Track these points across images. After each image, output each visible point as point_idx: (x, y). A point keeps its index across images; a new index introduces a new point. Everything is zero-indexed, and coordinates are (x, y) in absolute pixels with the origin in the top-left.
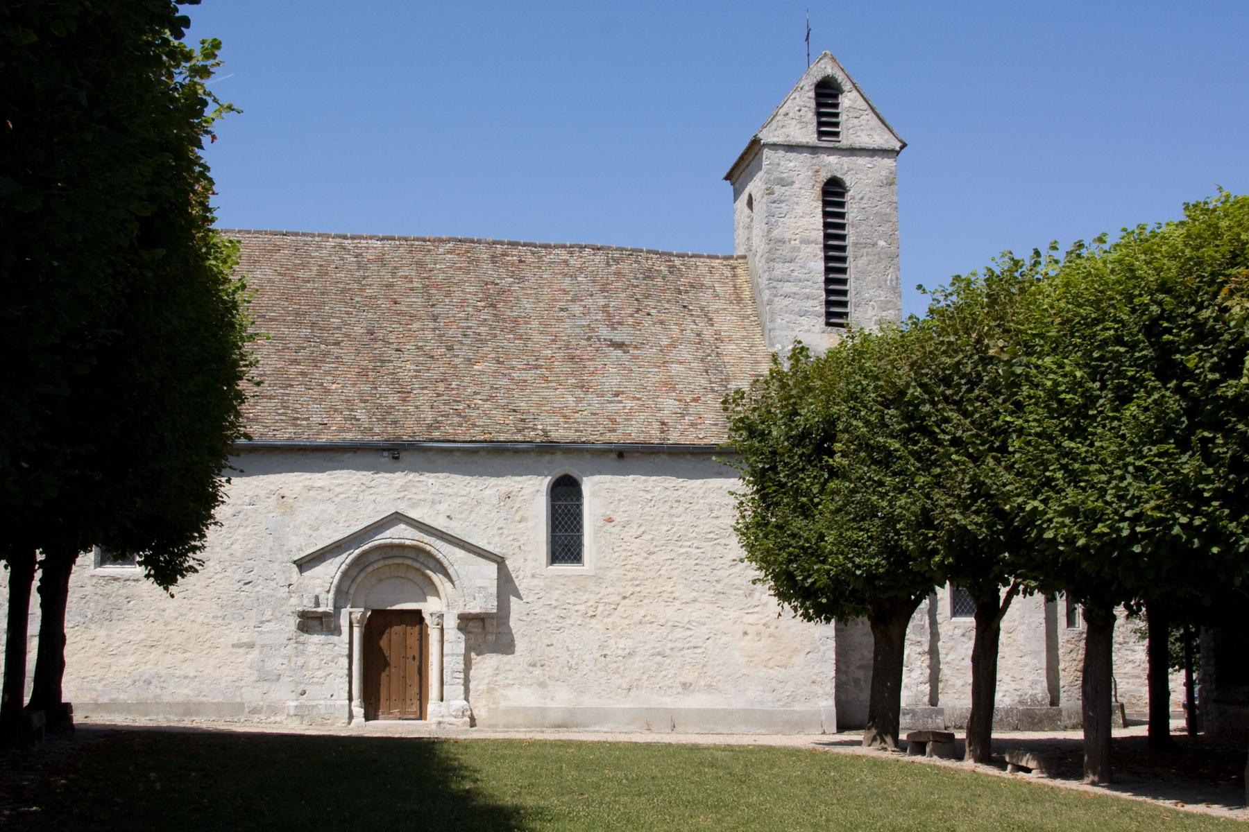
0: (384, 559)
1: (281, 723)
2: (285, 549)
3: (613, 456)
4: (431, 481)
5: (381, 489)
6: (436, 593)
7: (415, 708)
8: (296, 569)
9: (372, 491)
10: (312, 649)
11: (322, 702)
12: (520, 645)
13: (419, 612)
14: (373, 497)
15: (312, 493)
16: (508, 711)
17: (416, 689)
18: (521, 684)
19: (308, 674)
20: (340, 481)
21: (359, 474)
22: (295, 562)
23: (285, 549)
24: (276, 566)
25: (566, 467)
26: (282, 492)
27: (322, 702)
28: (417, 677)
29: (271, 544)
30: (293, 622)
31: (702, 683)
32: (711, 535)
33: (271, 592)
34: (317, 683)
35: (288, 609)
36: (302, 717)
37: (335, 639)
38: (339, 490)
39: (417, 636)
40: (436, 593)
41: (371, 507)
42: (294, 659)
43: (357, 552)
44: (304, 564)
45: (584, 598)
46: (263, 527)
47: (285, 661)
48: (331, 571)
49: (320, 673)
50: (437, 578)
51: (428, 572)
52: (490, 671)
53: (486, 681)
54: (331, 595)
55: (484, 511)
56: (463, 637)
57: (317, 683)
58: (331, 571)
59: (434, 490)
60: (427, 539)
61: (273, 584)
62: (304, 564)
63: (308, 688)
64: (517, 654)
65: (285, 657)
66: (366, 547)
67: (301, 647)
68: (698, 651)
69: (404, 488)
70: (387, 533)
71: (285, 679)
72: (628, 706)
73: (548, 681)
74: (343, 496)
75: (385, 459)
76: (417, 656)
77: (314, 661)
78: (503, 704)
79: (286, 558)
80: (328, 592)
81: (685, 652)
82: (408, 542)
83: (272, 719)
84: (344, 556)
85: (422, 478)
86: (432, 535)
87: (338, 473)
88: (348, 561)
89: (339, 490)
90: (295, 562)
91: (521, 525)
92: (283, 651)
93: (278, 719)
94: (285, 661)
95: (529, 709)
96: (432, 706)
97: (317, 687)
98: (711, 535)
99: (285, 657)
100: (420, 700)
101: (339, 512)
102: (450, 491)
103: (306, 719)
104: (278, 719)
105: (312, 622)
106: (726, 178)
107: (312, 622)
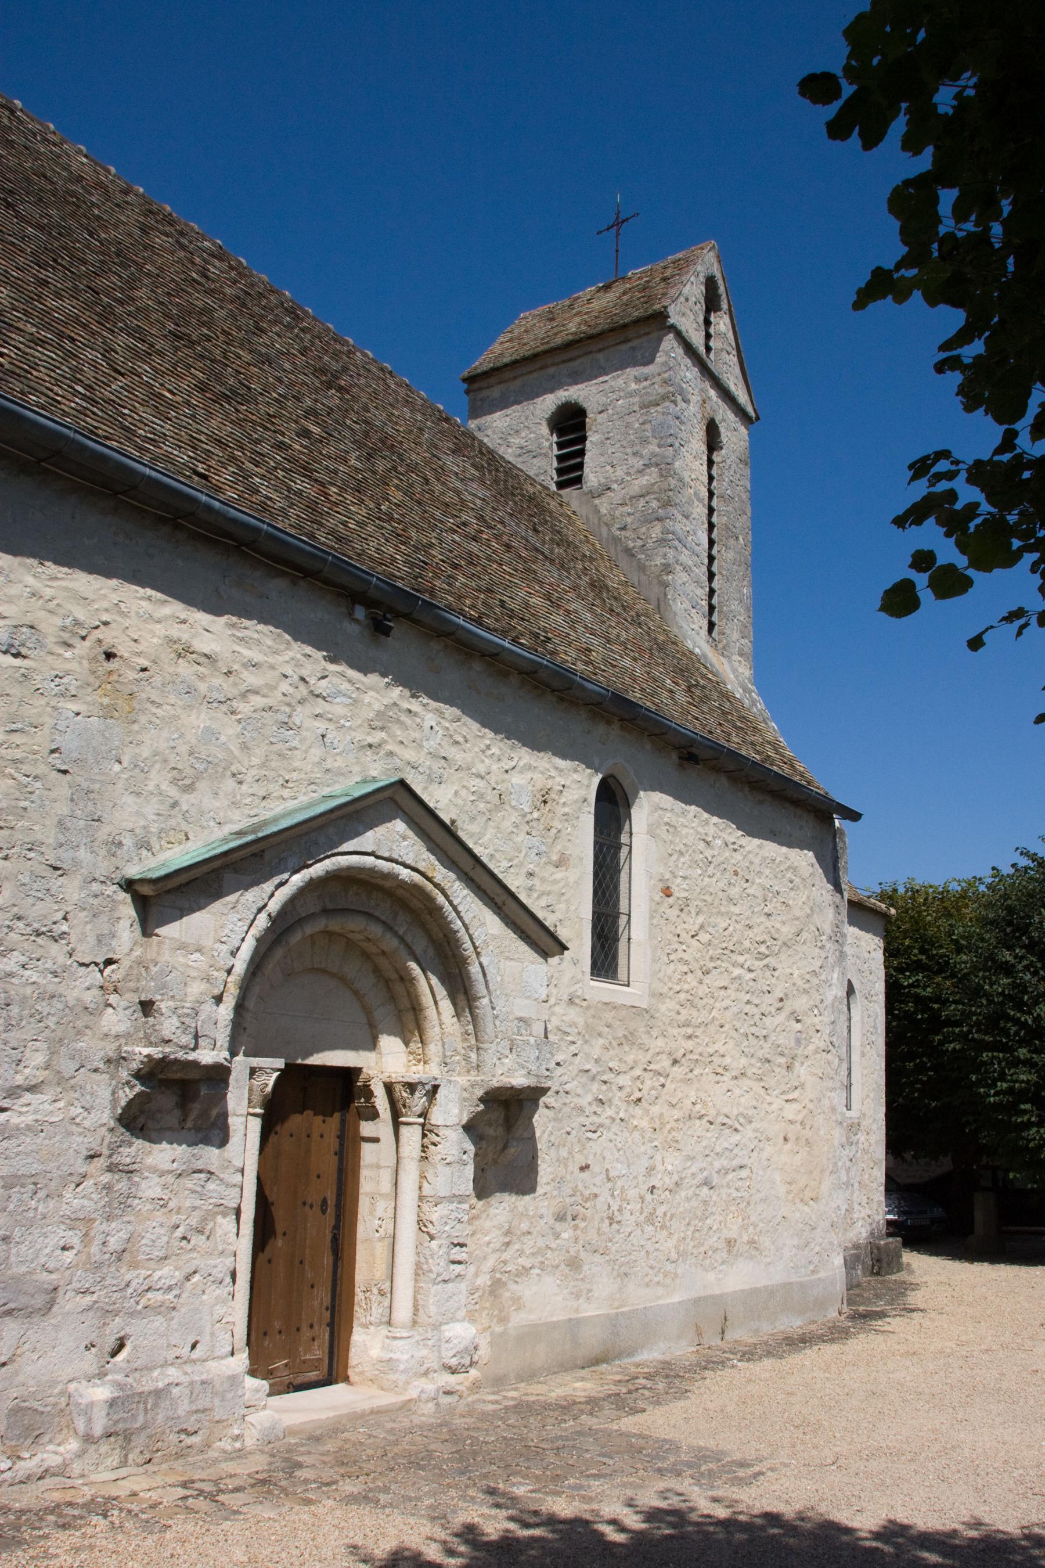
0: (326, 912)
1: (61, 1471)
2: (103, 832)
3: (674, 756)
4: (430, 719)
5: (338, 708)
6: (409, 1022)
7: (318, 1352)
8: (128, 911)
9: (321, 707)
10: (151, 1188)
11: (173, 1373)
12: (545, 1171)
13: (349, 1074)
14: (321, 726)
15: (185, 669)
16: (533, 1334)
17: (323, 1295)
18: (542, 1266)
19: (137, 1277)
20: (257, 656)
21: (298, 650)
22: (129, 885)
23: (103, 832)
24: (72, 889)
25: (628, 757)
26: (109, 637)
27: (173, 1373)
28: (327, 1260)
29: (63, 809)
30: (106, 1097)
31: (745, 1238)
32: (763, 949)
33: (49, 983)
34: (157, 1309)
35: (98, 1050)
36: (127, 1436)
37: (210, 1155)
38: (252, 679)
39: (332, 1142)
40: (409, 1022)
41: (316, 753)
42: (100, 1227)
43: (298, 880)
44: (160, 900)
45: (630, 1058)
46: (41, 740)
47: (74, 1238)
48: (227, 932)
49: (167, 1274)
50: (429, 987)
51: (413, 965)
52: (496, 1238)
53: (490, 1263)
54: (225, 1012)
55: (507, 825)
56: (471, 1148)
57: (157, 1309)
58: (227, 932)
59: (431, 745)
60: (442, 874)
61: (57, 951)
62: (160, 900)
63: (135, 1329)
64: (540, 1190)
65: (73, 1221)
66: (318, 870)
67: (122, 1185)
68: (744, 1173)
69: (382, 721)
70: (368, 840)
71: (69, 1303)
72: (676, 1299)
73: (583, 1255)
74: (257, 701)
75: (353, 628)
76: (331, 1202)
77: (154, 1233)
78: (518, 1319)
79: (104, 867)
80: (218, 999)
81: (730, 1176)
82: (405, 874)
83: (28, 1465)
84: (268, 886)
85: (415, 706)
86: (450, 863)
87: (253, 629)
88: (274, 906)
89: (252, 679)
90: (129, 885)
91: (559, 875)
92: (73, 1201)
93: (49, 1455)
94: (74, 1238)
95: (554, 1326)
96: (366, 1344)
97: (159, 1322)
98: (763, 949)
99: (73, 1221)
100: (331, 1325)
101: (245, 747)
102: (457, 755)
103: (139, 1441)
104: (49, 1455)
105: (173, 1099)
106: (464, 380)
107: (173, 1099)
